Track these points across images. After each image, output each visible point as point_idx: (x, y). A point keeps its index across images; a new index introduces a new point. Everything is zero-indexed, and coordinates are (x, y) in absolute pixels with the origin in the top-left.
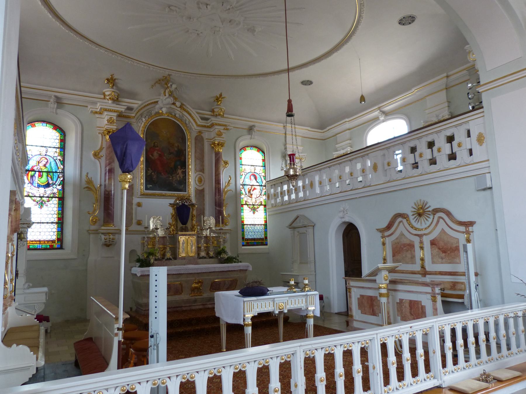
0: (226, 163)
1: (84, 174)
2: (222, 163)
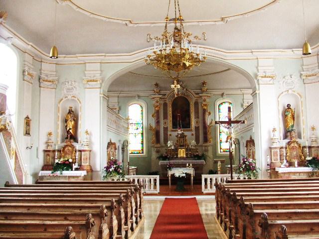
0: (210, 113)
1: (149, 124)
2: (207, 113)
